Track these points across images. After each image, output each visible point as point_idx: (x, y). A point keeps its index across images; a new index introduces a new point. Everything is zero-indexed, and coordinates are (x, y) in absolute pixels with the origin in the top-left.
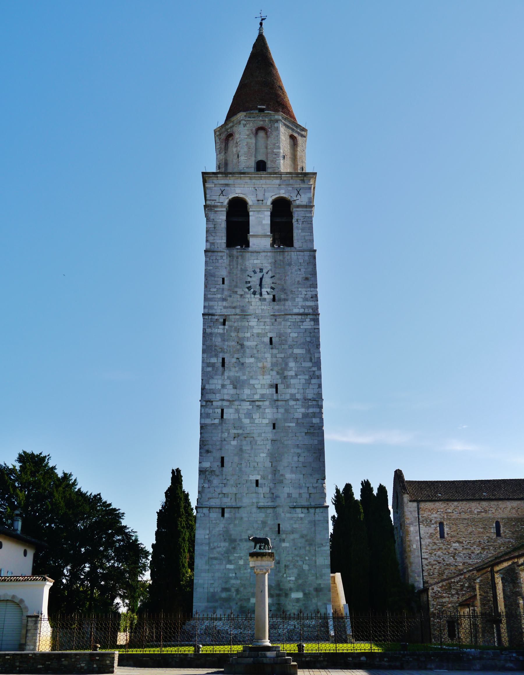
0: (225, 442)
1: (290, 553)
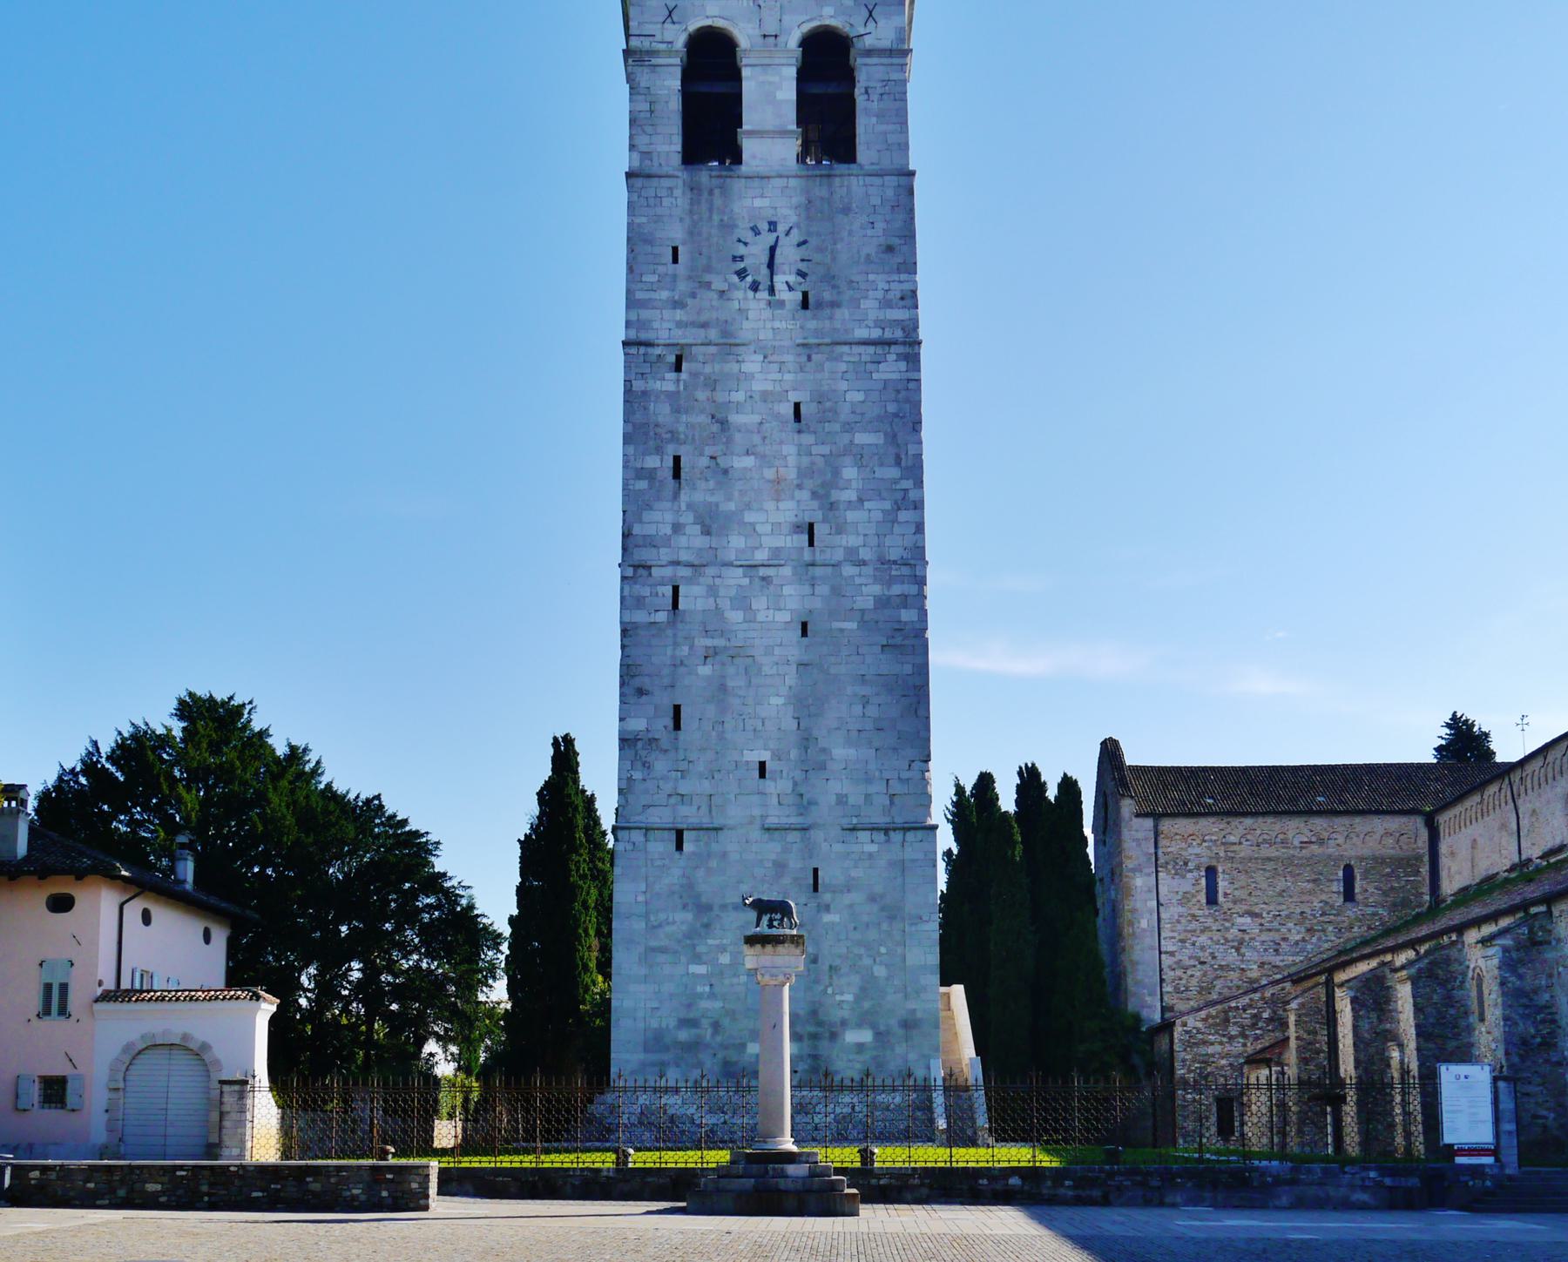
0: (682, 670)
1: (843, 937)
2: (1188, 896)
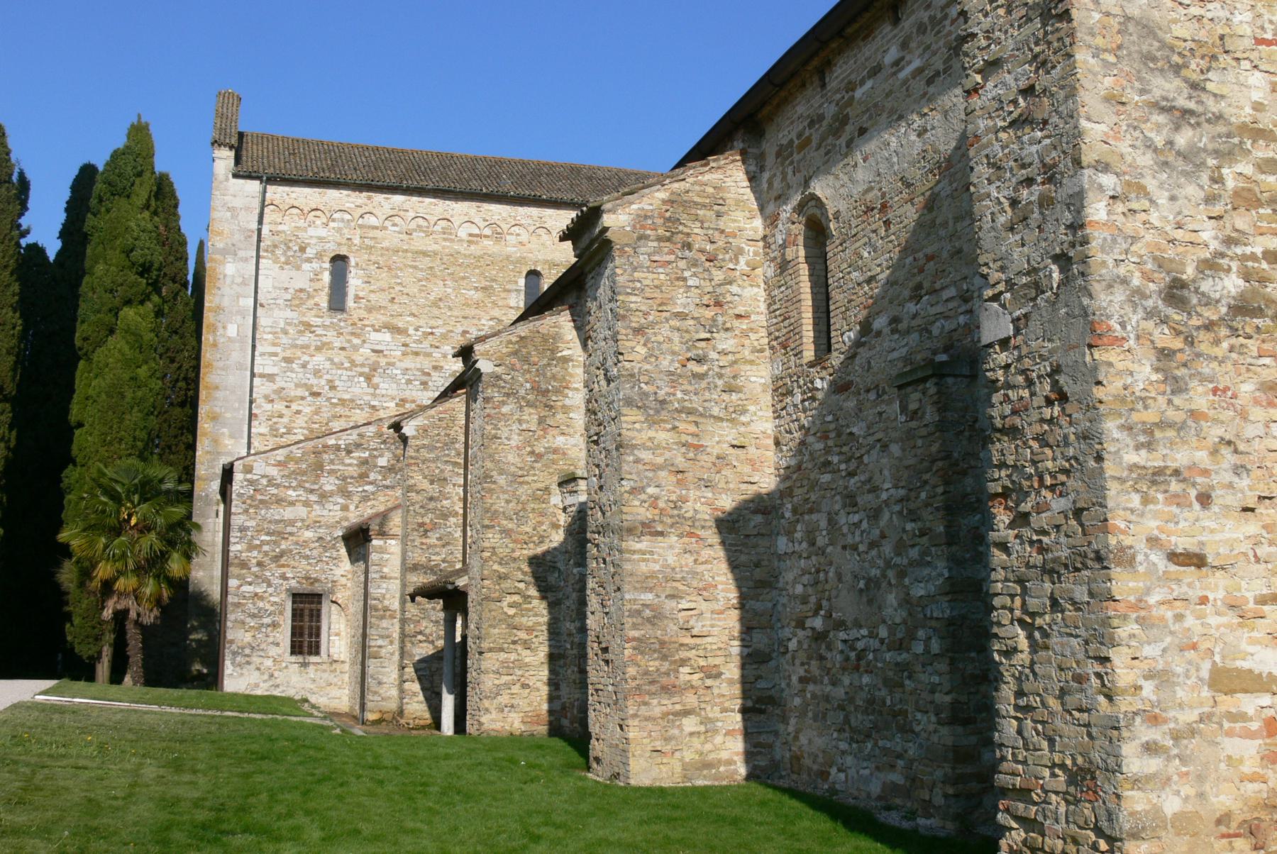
2: (302, 295)
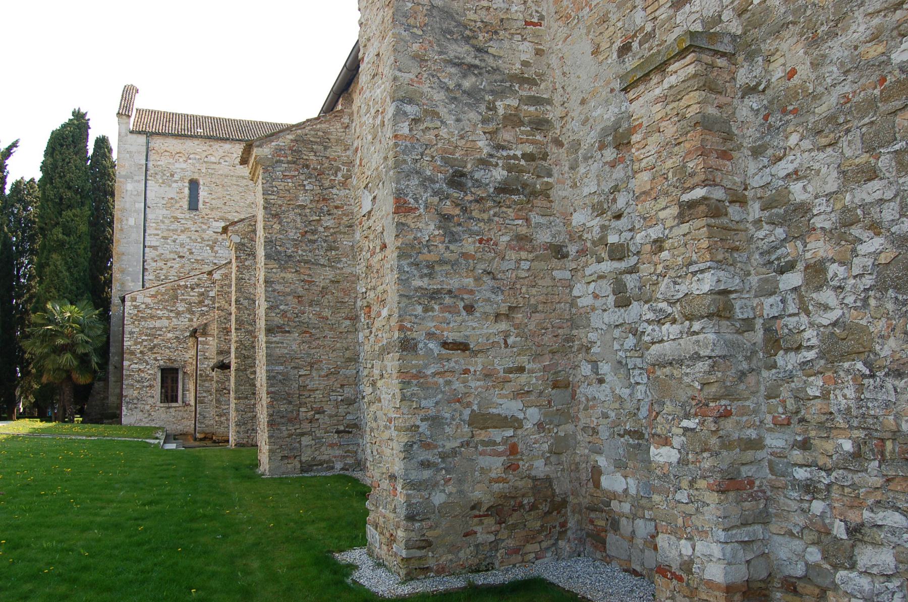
2: (172, 201)
